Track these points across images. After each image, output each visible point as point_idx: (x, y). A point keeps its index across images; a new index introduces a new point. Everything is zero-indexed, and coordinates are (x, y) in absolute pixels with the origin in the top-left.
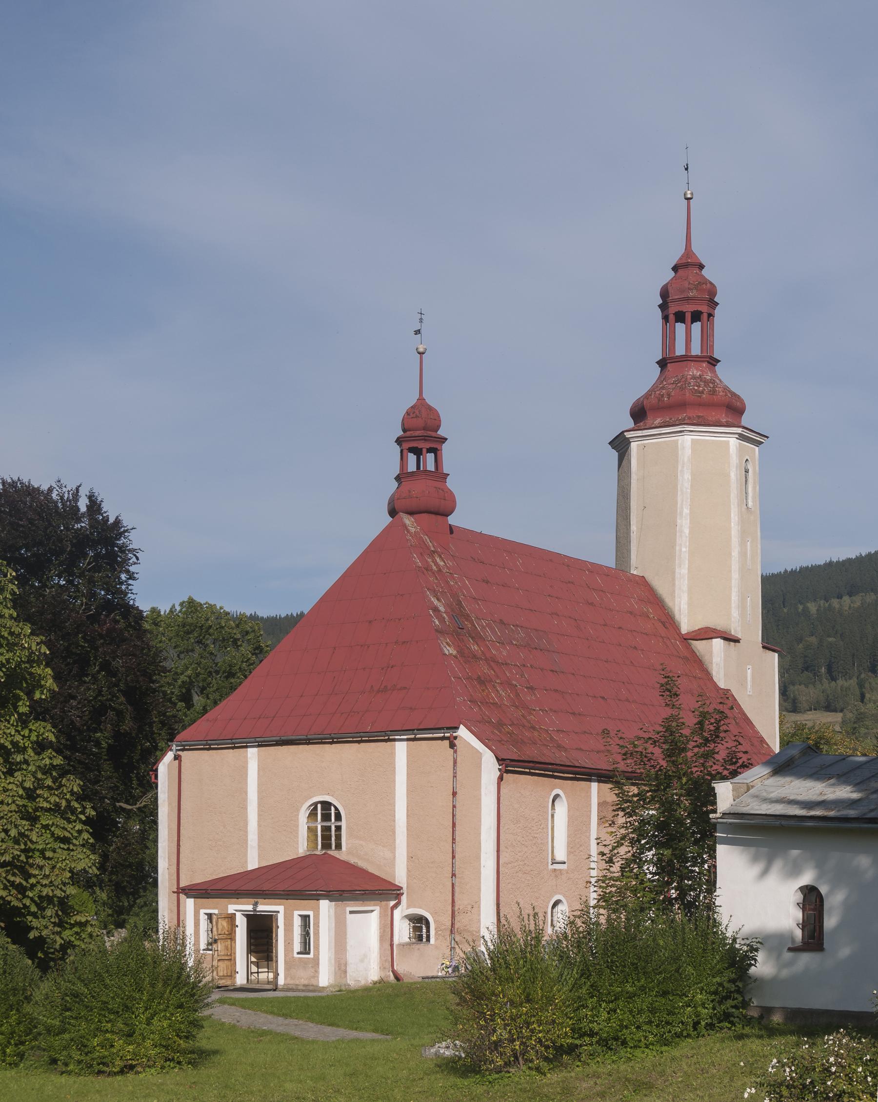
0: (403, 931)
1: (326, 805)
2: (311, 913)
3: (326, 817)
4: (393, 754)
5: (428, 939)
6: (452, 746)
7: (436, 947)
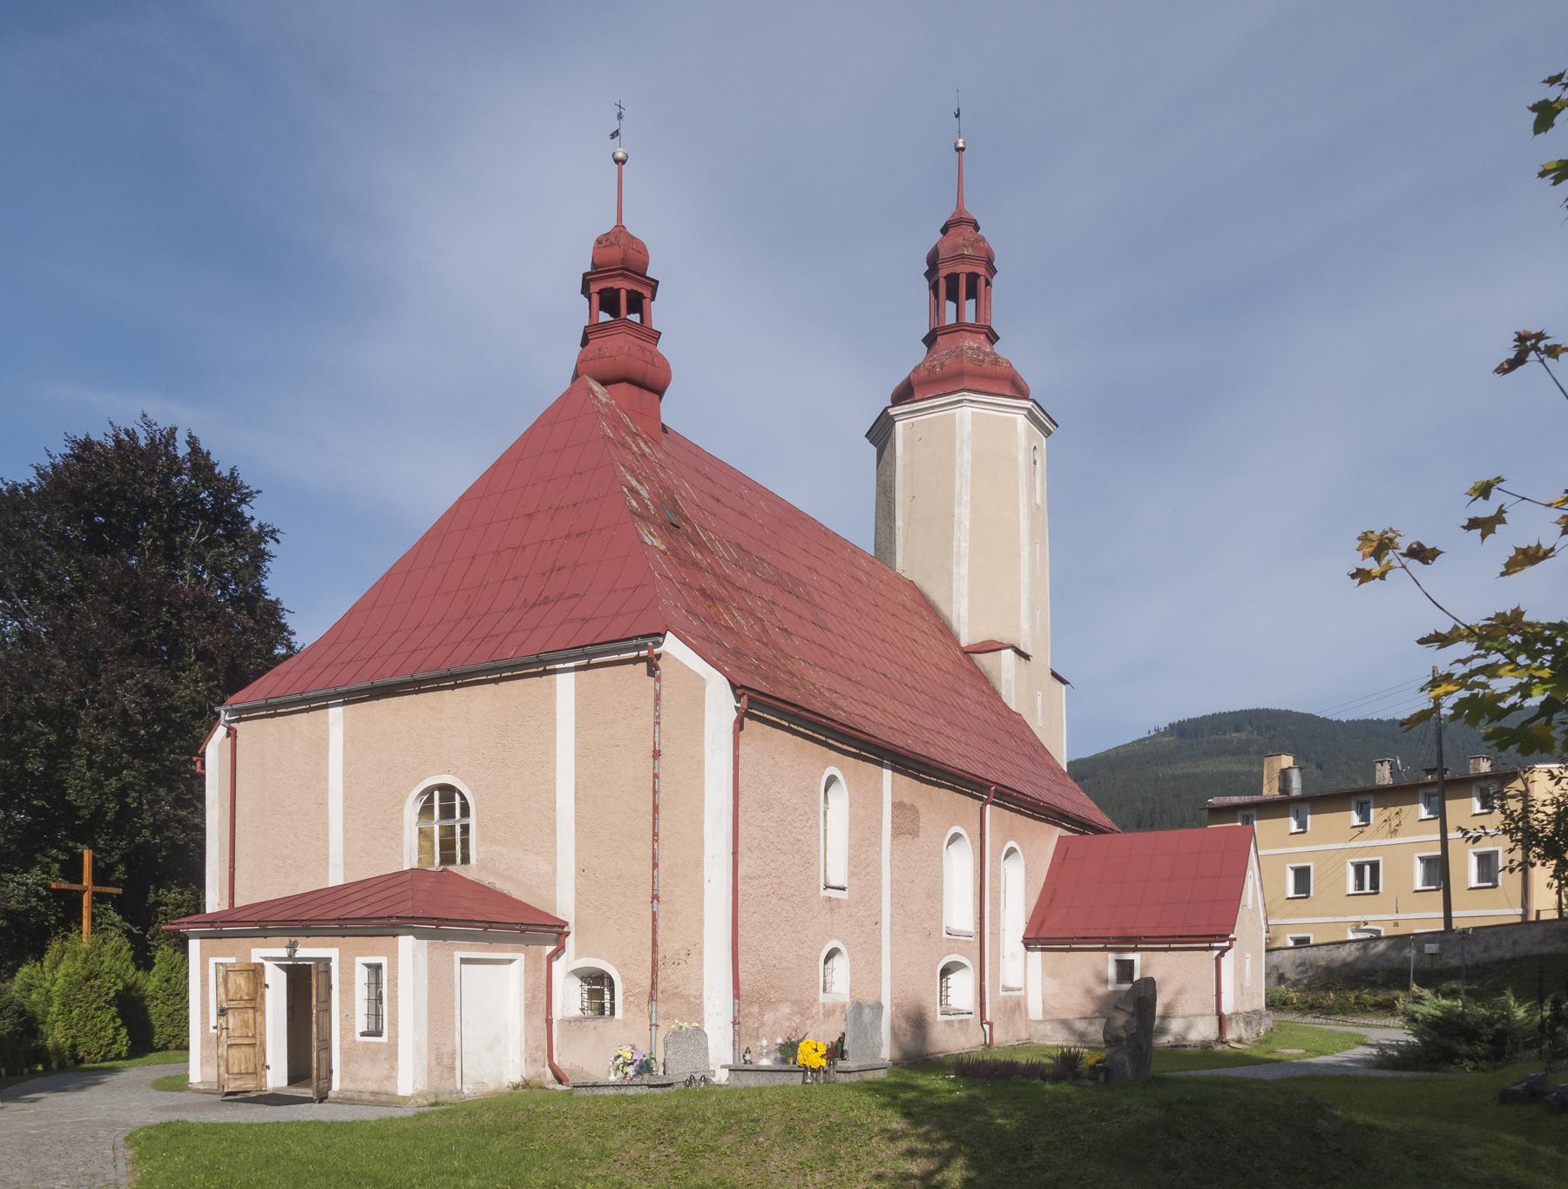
0: (569, 997)
1: (447, 791)
2: (383, 960)
3: (447, 812)
4: (551, 696)
5: (612, 1013)
6: (653, 670)
7: (625, 1025)
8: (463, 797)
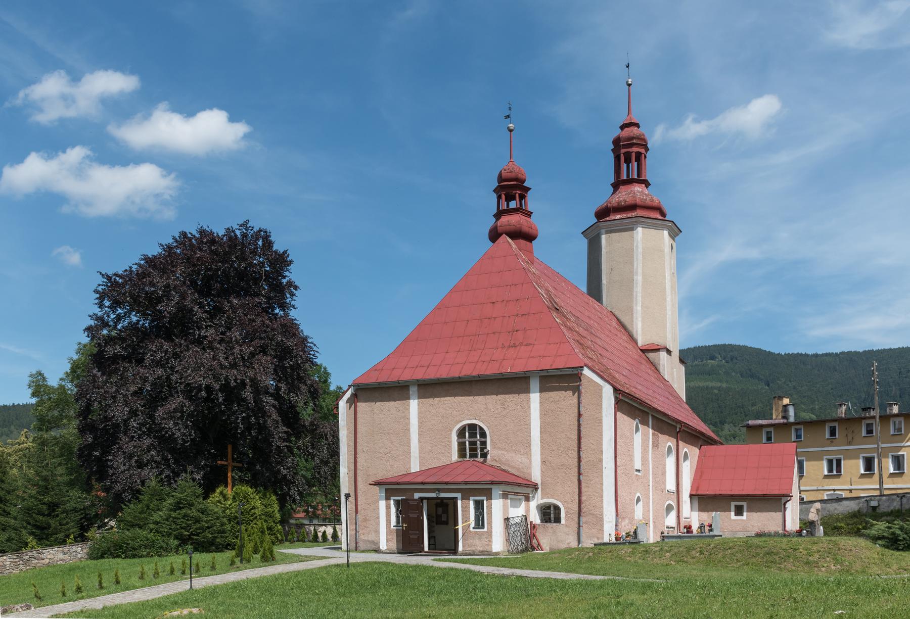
1: (472, 427)
3: (473, 435)
8: (481, 428)
